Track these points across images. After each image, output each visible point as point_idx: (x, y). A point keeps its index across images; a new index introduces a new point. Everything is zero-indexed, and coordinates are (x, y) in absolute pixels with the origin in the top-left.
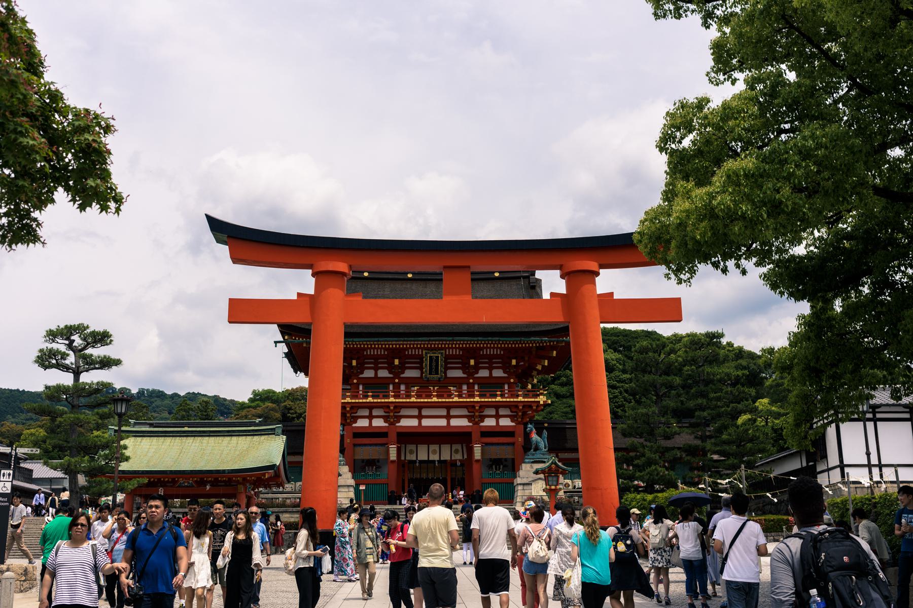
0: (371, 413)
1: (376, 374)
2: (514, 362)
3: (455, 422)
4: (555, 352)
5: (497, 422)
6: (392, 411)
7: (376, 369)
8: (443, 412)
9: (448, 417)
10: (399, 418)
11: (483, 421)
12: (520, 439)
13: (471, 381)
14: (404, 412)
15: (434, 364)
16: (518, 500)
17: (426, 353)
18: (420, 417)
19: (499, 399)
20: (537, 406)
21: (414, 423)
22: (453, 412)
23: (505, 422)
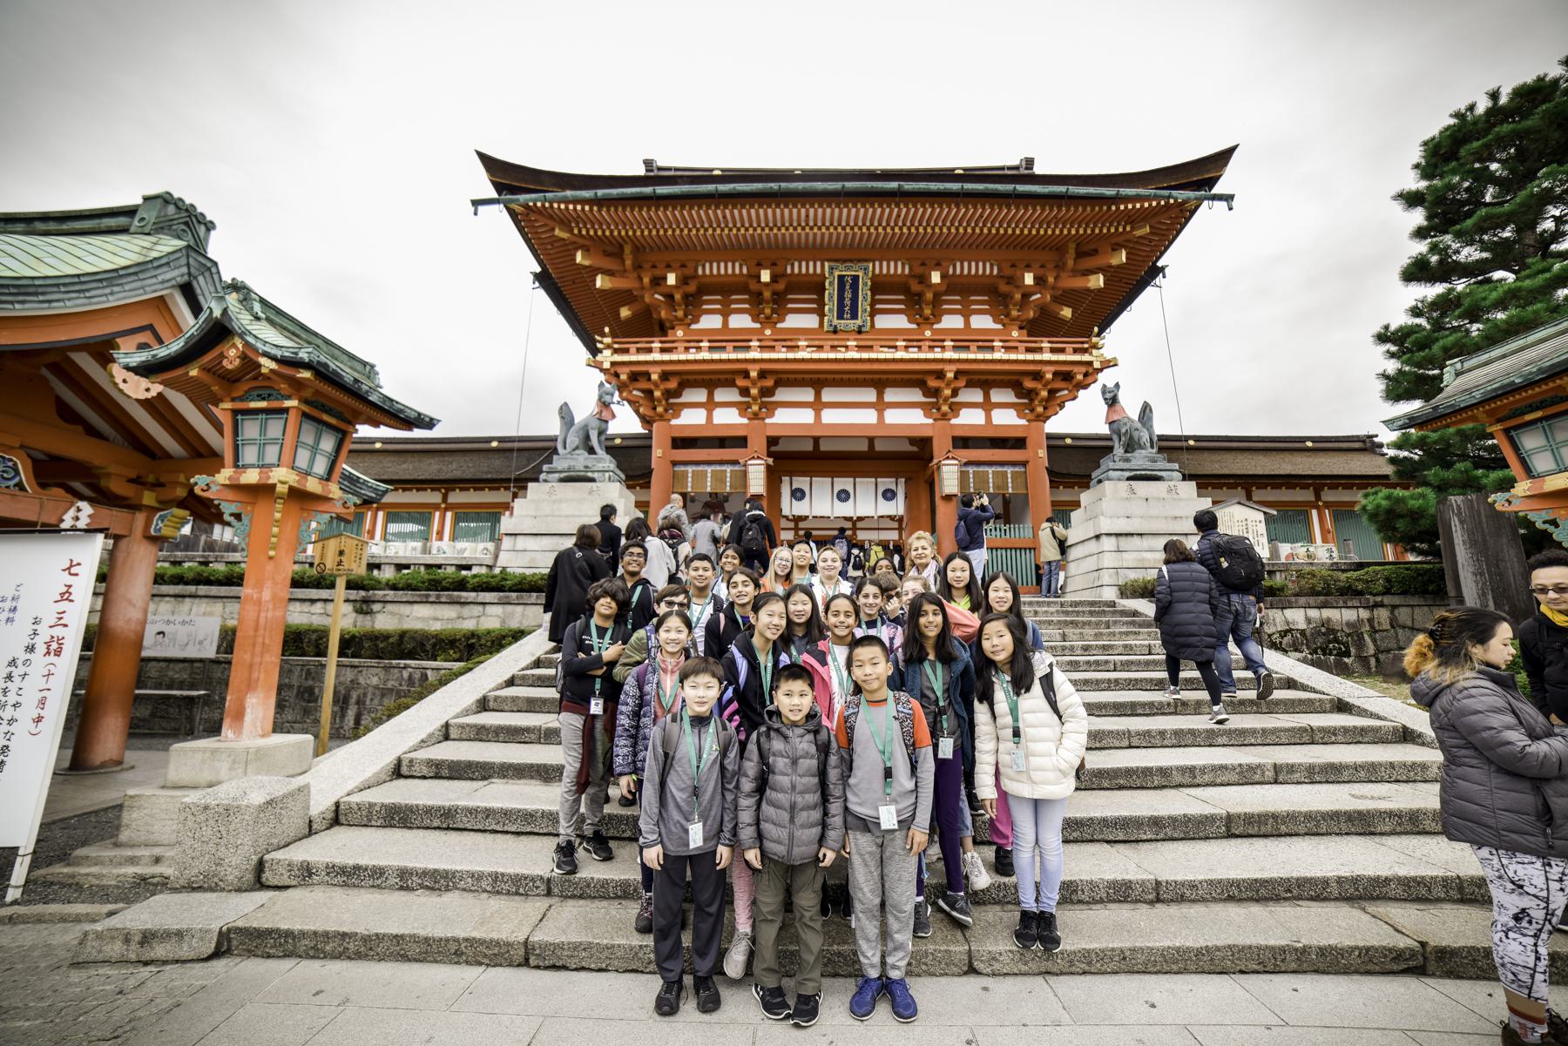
0: (711, 395)
1: (725, 323)
2: (1029, 279)
3: (894, 417)
4: (1124, 253)
5: (988, 418)
6: (754, 383)
7: (726, 315)
8: (870, 395)
9: (880, 406)
10: (771, 408)
11: (957, 416)
12: (1043, 453)
13: (928, 334)
14: (782, 395)
15: (848, 295)
16: (1107, 577)
17: (832, 268)
18: (818, 406)
19: (997, 355)
20: (1086, 375)
21: (805, 417)
22: (891, 395)
23: (1007, 419)
